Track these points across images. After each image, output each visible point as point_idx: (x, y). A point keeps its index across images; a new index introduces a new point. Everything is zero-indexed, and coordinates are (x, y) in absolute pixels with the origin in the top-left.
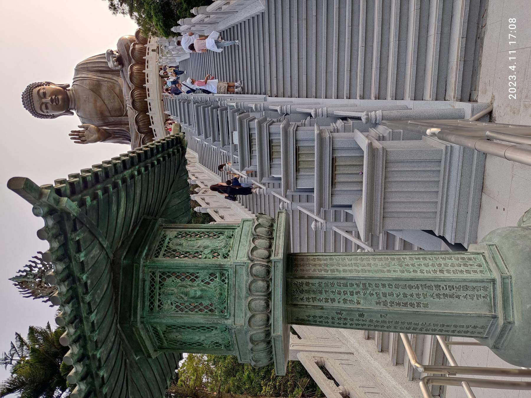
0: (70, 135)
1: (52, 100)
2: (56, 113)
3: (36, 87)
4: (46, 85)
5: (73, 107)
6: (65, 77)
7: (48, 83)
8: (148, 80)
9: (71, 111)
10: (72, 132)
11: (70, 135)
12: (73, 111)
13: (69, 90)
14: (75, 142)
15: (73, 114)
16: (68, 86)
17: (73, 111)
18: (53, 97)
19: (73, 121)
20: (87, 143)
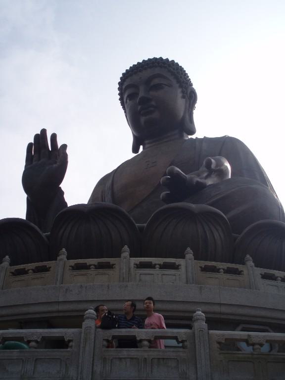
0: (44, 132)
1: (145, 101)
3: (173, 74)
4: (183, 92)
5: (147, 146)
6: (207, 123)
9: (141, 147)
11: (44, 132)
13: (182, 136)
14: (30, 145)
15: (135, 149)
16: (192, 132)
18: (153, 103)
20: (26, 166)
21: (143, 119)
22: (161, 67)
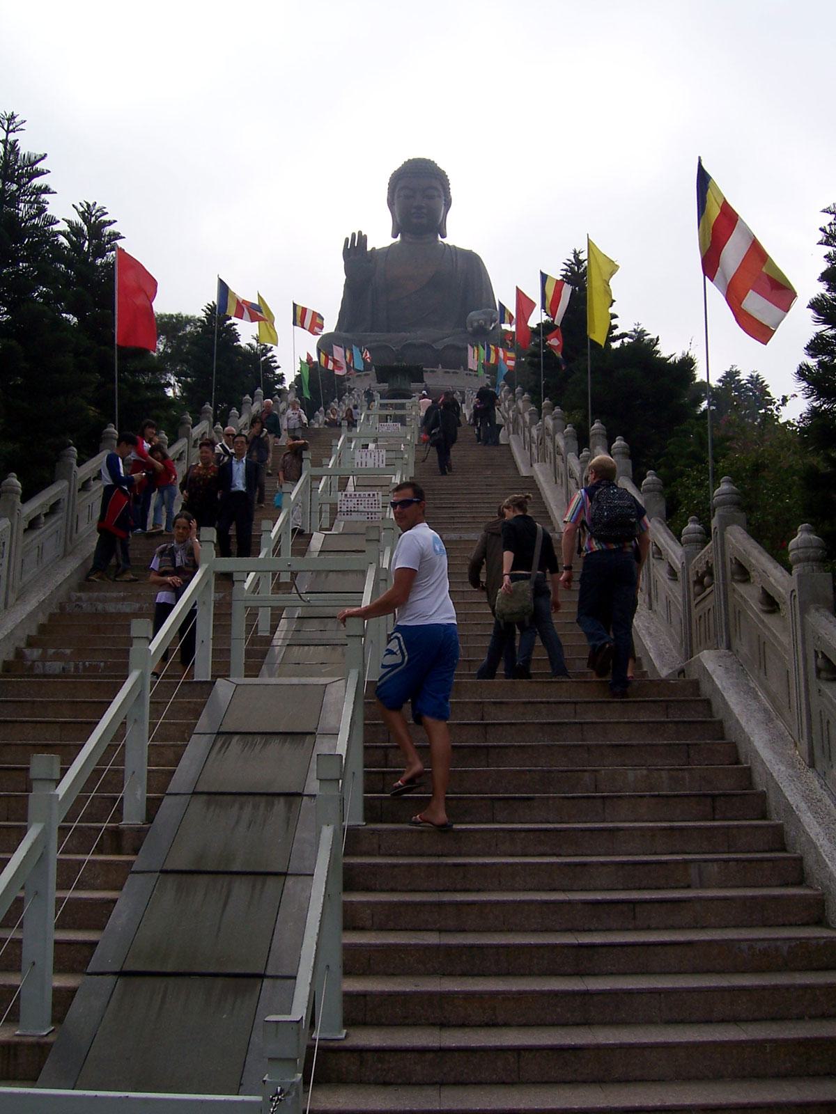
0: (360, 233)
2: (396, 208)
3: (442, 184)
4: (445, 200)
7: (448, 204)
8: (449, 372)
10: (365, 236)
12: (399, 238)
14: (347, 239)
15: (395, 236)
16: (444, 236)
17: (399, 238)
18: (425, 211)
19: (381, 236)
21: (415, 221)
22: (436, 178)
